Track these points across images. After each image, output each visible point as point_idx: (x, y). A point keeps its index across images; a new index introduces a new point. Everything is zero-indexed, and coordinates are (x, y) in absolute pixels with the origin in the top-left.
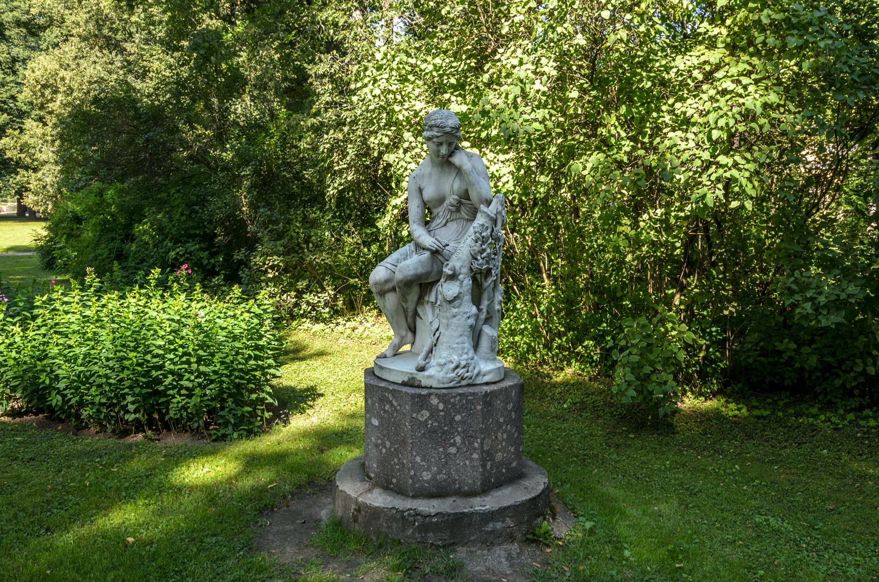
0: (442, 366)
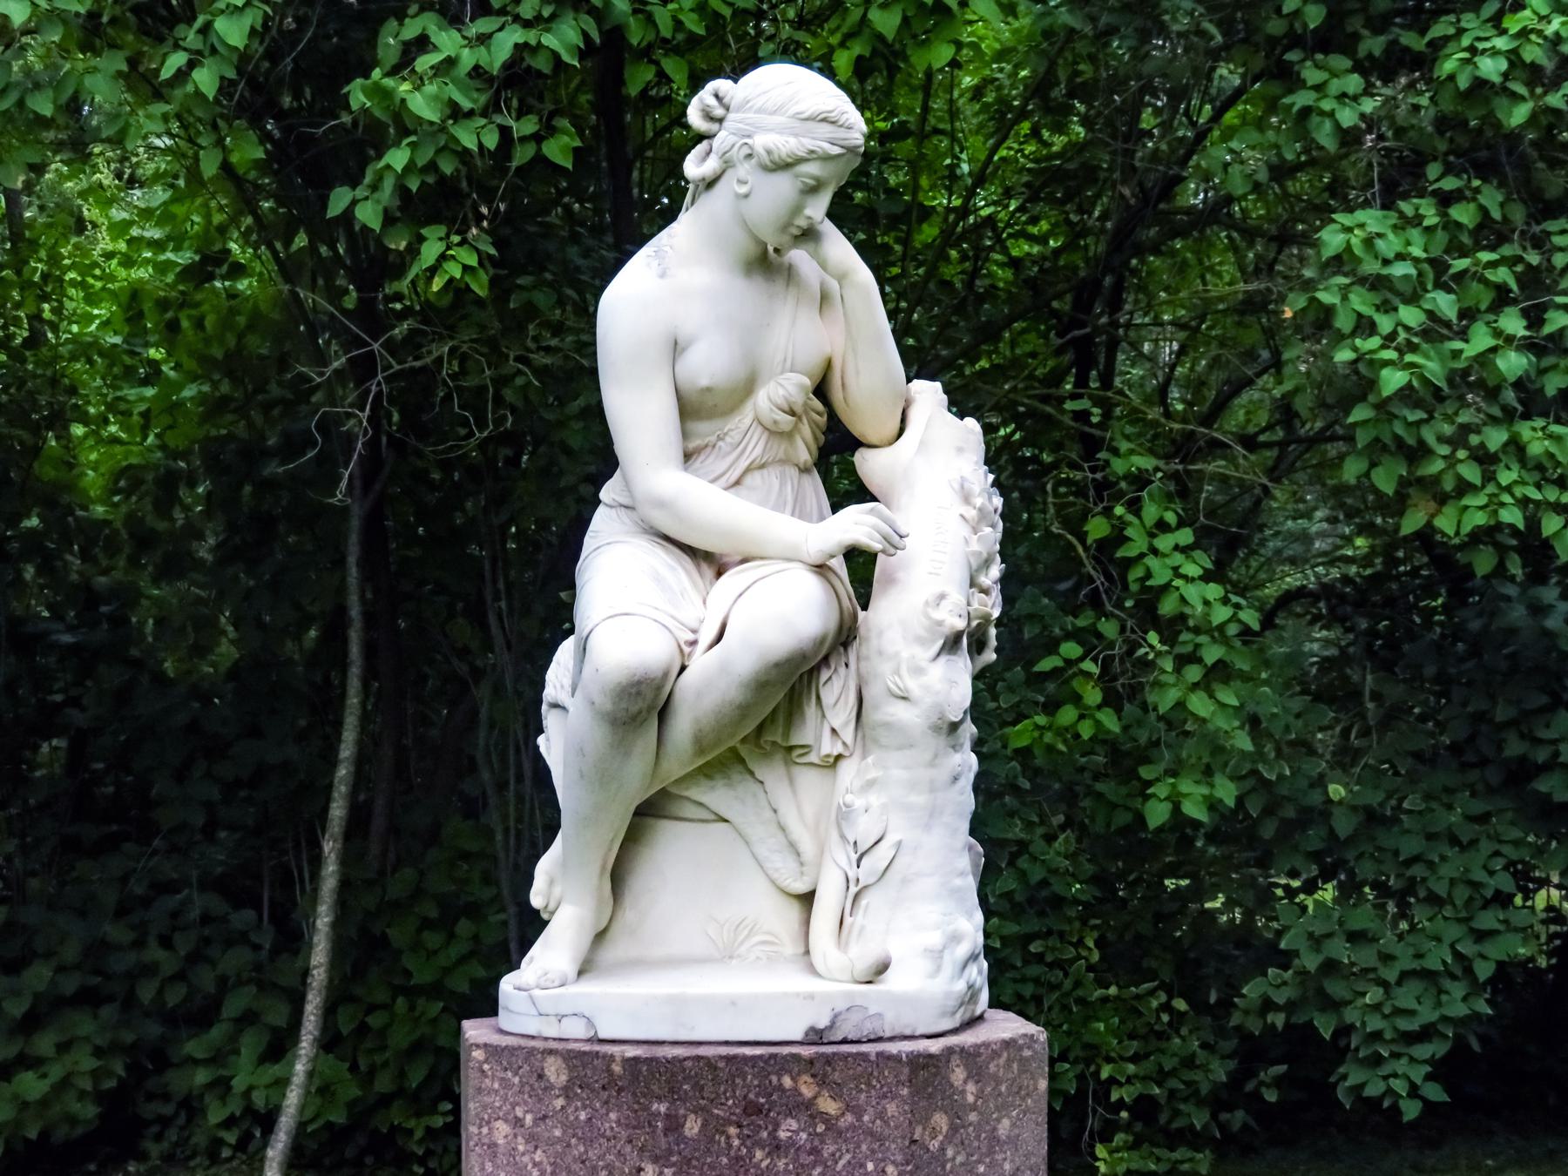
0: (937, 955)
